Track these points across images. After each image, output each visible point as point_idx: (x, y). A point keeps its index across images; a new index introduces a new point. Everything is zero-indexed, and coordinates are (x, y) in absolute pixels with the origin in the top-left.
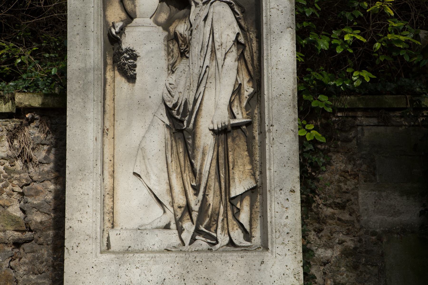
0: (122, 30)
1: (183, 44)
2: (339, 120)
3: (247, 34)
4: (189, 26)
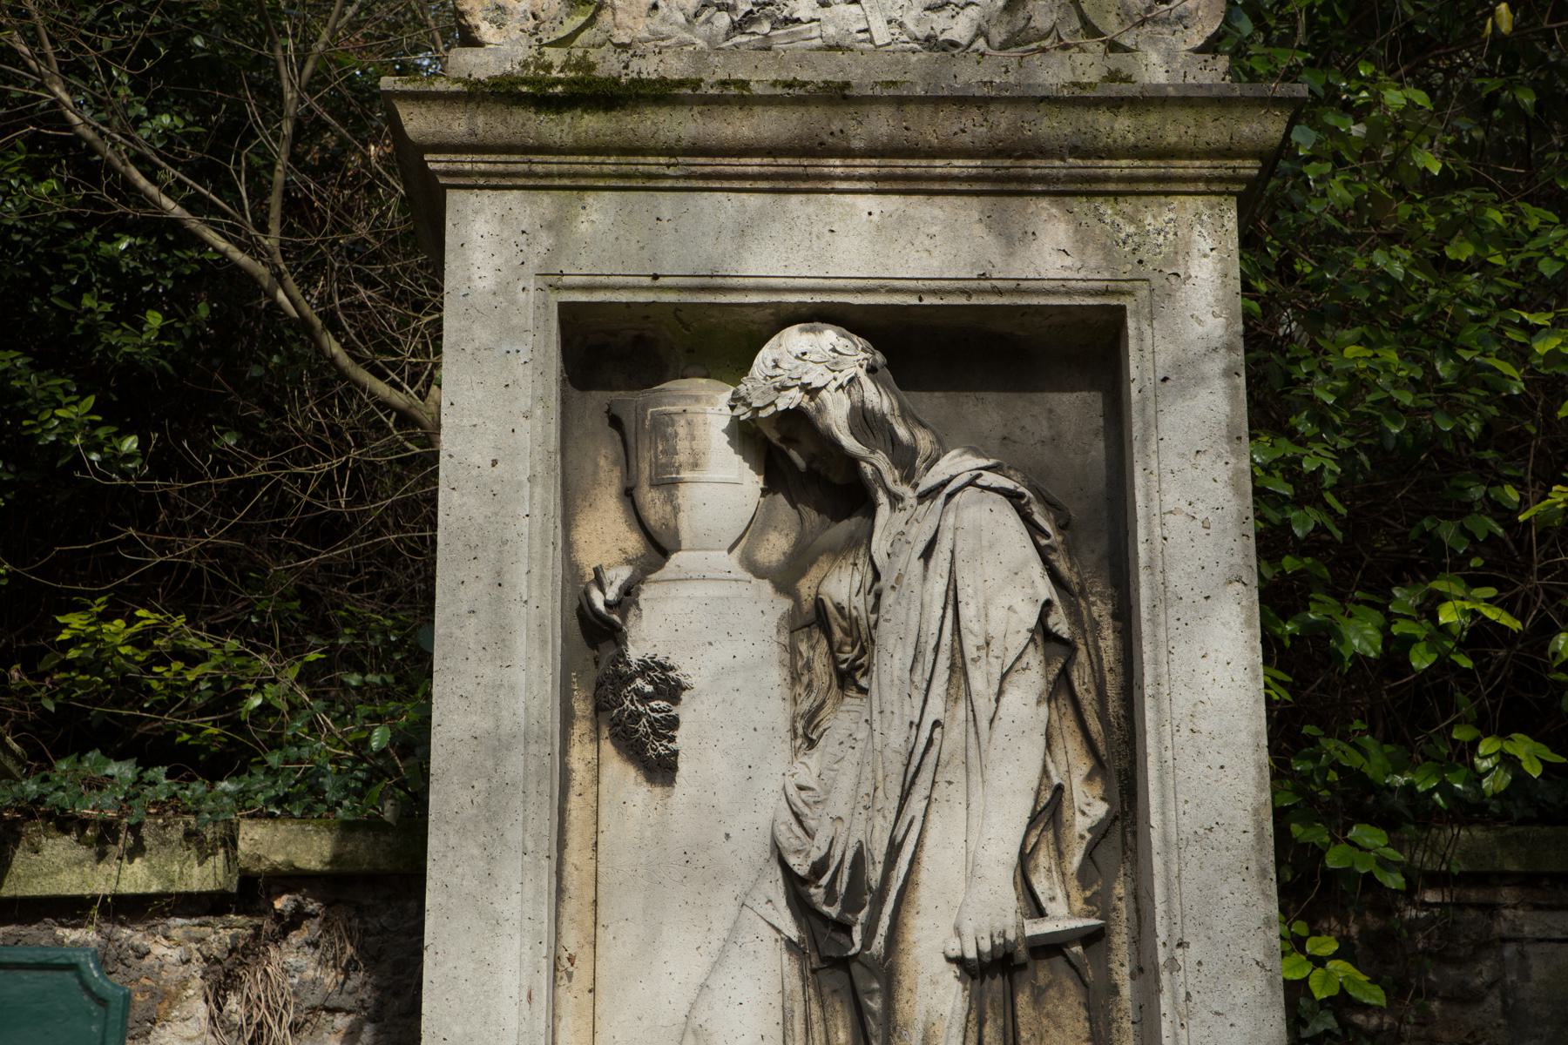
0: (629, 592)
1: (849, 640)
2: (1431, 921)
3: (1078, 605)
4: (869, 577)
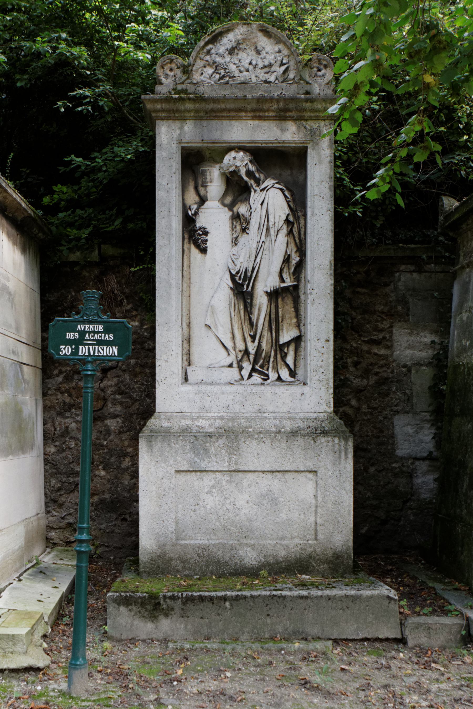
0: (196, 214)
